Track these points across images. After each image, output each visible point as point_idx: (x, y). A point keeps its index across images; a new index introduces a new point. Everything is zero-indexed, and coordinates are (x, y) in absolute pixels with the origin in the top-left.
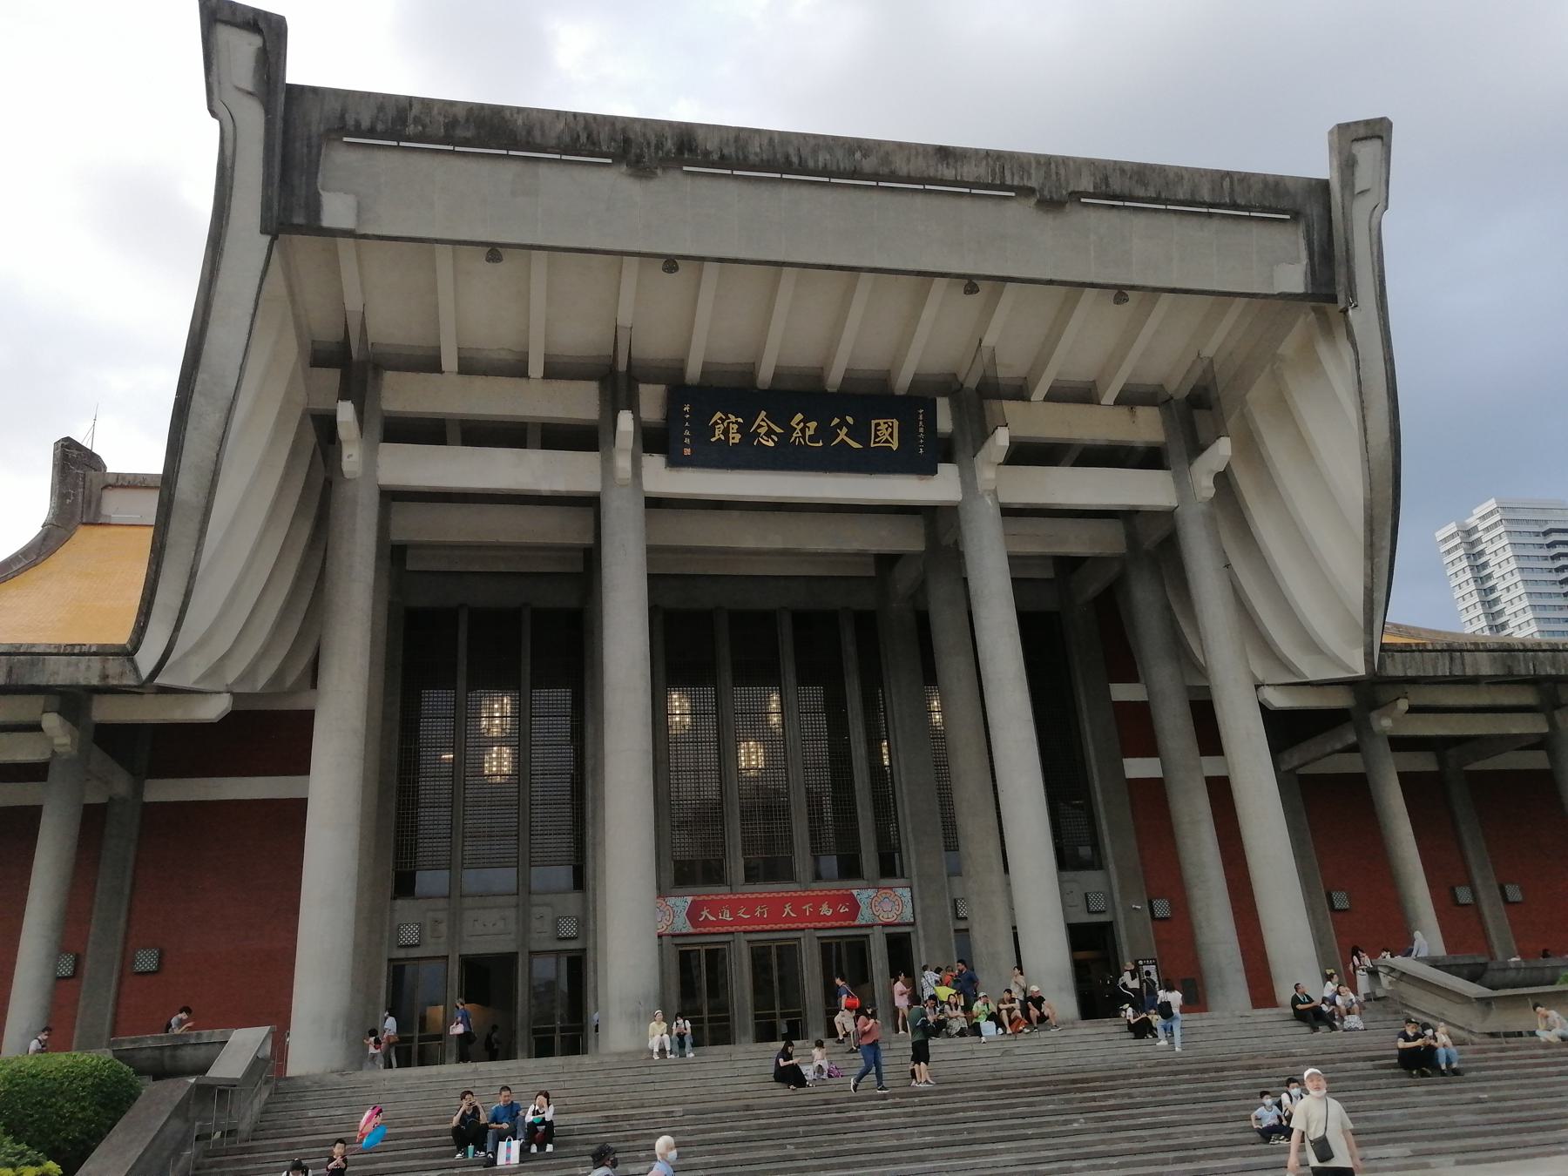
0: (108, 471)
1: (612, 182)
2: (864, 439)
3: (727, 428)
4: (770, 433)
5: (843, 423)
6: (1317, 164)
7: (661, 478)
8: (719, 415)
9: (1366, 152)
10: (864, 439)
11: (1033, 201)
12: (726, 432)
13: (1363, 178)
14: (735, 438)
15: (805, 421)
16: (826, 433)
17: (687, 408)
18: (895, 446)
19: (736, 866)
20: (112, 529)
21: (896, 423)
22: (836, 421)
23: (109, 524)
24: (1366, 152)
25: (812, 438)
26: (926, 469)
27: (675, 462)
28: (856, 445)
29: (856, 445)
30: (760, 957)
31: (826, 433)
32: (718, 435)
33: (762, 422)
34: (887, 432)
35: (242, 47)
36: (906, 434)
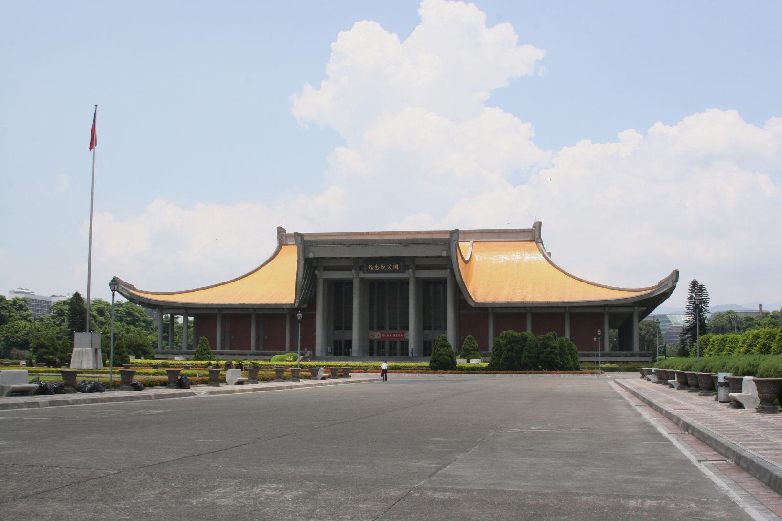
2: (392, 268)
3: (371, 267)
4: (378, 268)
7: (363, 275)
10: (392, 268)
13: (453, 238)
14: (372, 269)
16: (386, 267)
19: (387, 327)
26: (404, 272)
27: (364, 273)
30: (390, 342)
31: (386, 267)
34: (396, 267)
35: (299, 238)
36: (400, 267)
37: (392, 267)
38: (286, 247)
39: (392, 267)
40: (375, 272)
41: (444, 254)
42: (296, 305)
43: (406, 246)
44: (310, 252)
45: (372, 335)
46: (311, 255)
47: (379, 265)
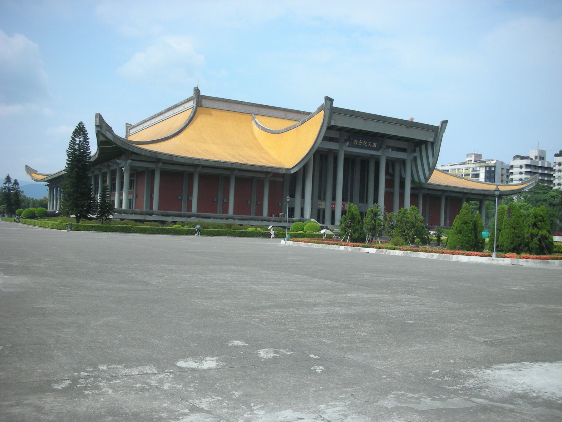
0: (201, 94)
1: (361, 120)
3: (356, 142)
5: (370, 143)
6: (437, 124)
8: (355, 140)
9: (444, 124)
11: (406, 126)
12: (356, 143)
14: (357, 144)
15: (365, 142)
16: (368, 144)
17: (352, 139)
18: (375, 147)
20: (204, 108)
21: (376, 143)
22: (369, 143)
23: (203, 107)
24: (444, 124)
25: (366, 145)
28: (371, 146)
29: (371, 146)
31: (368, 144)
32: (355, 143)
33: (360, 142)
34: (375, 145)
37: (372, 145)
38: (201, 108)
39: (372, 145)
40: (358, 146)
41: (431, 140)
42: (292, 172)
43: (408, 127)
44: (332, 120)
45: (319, 205)
46: (333, 123)
47: (363, 142)
